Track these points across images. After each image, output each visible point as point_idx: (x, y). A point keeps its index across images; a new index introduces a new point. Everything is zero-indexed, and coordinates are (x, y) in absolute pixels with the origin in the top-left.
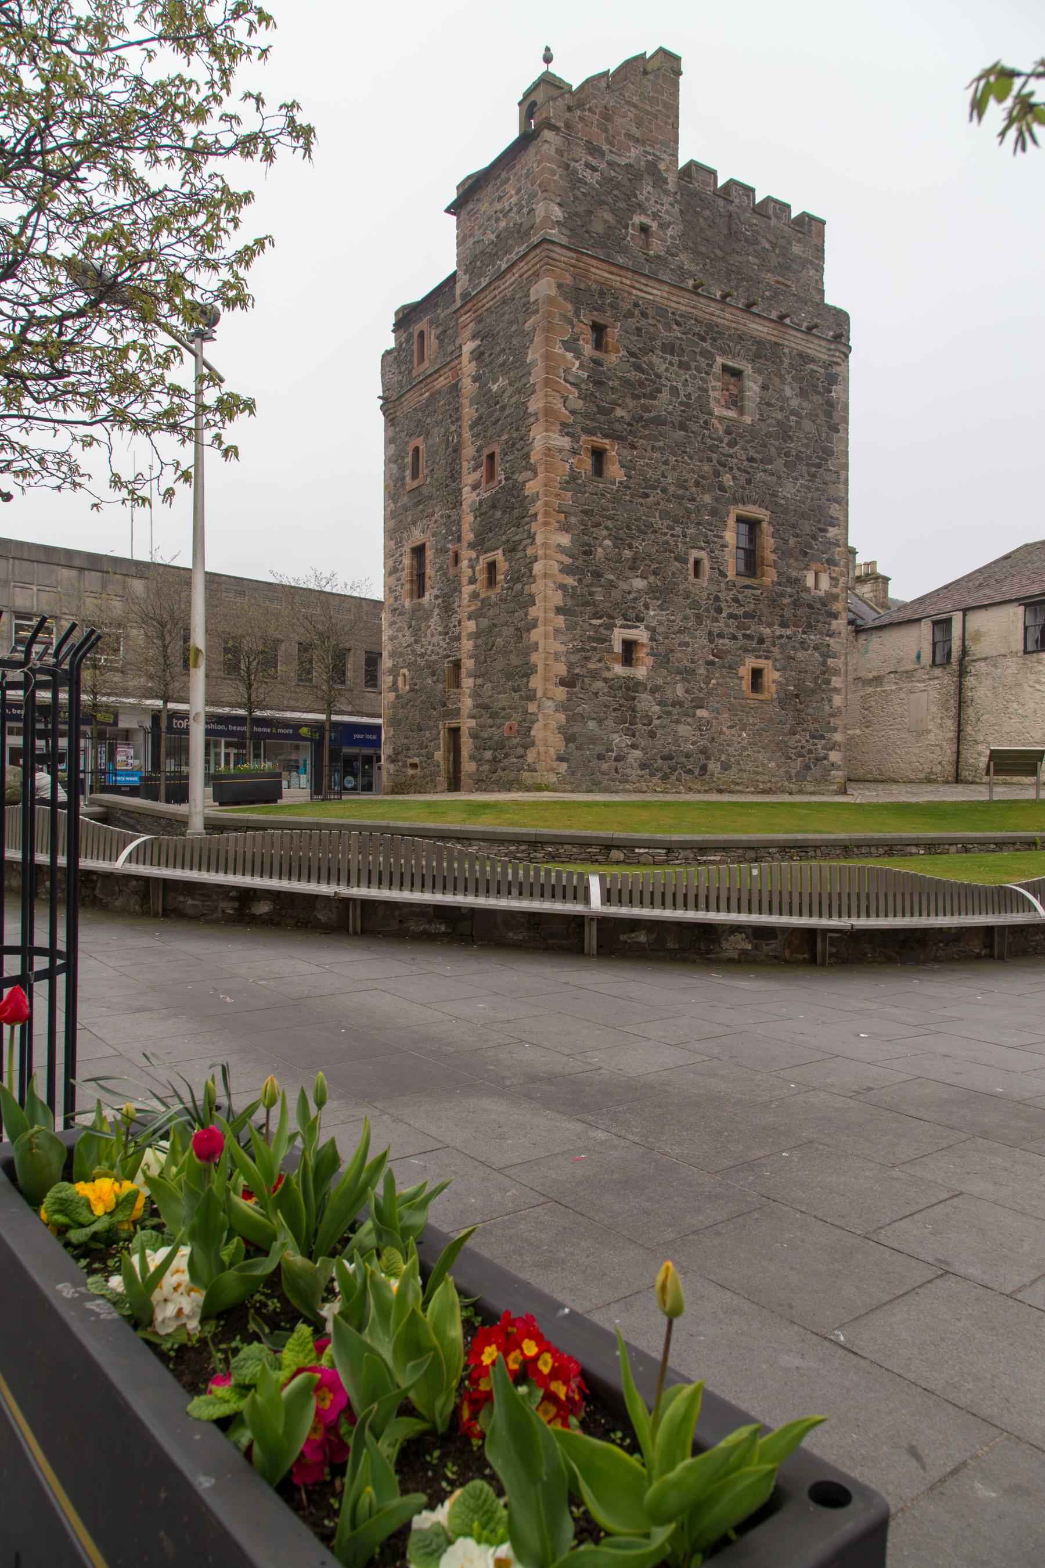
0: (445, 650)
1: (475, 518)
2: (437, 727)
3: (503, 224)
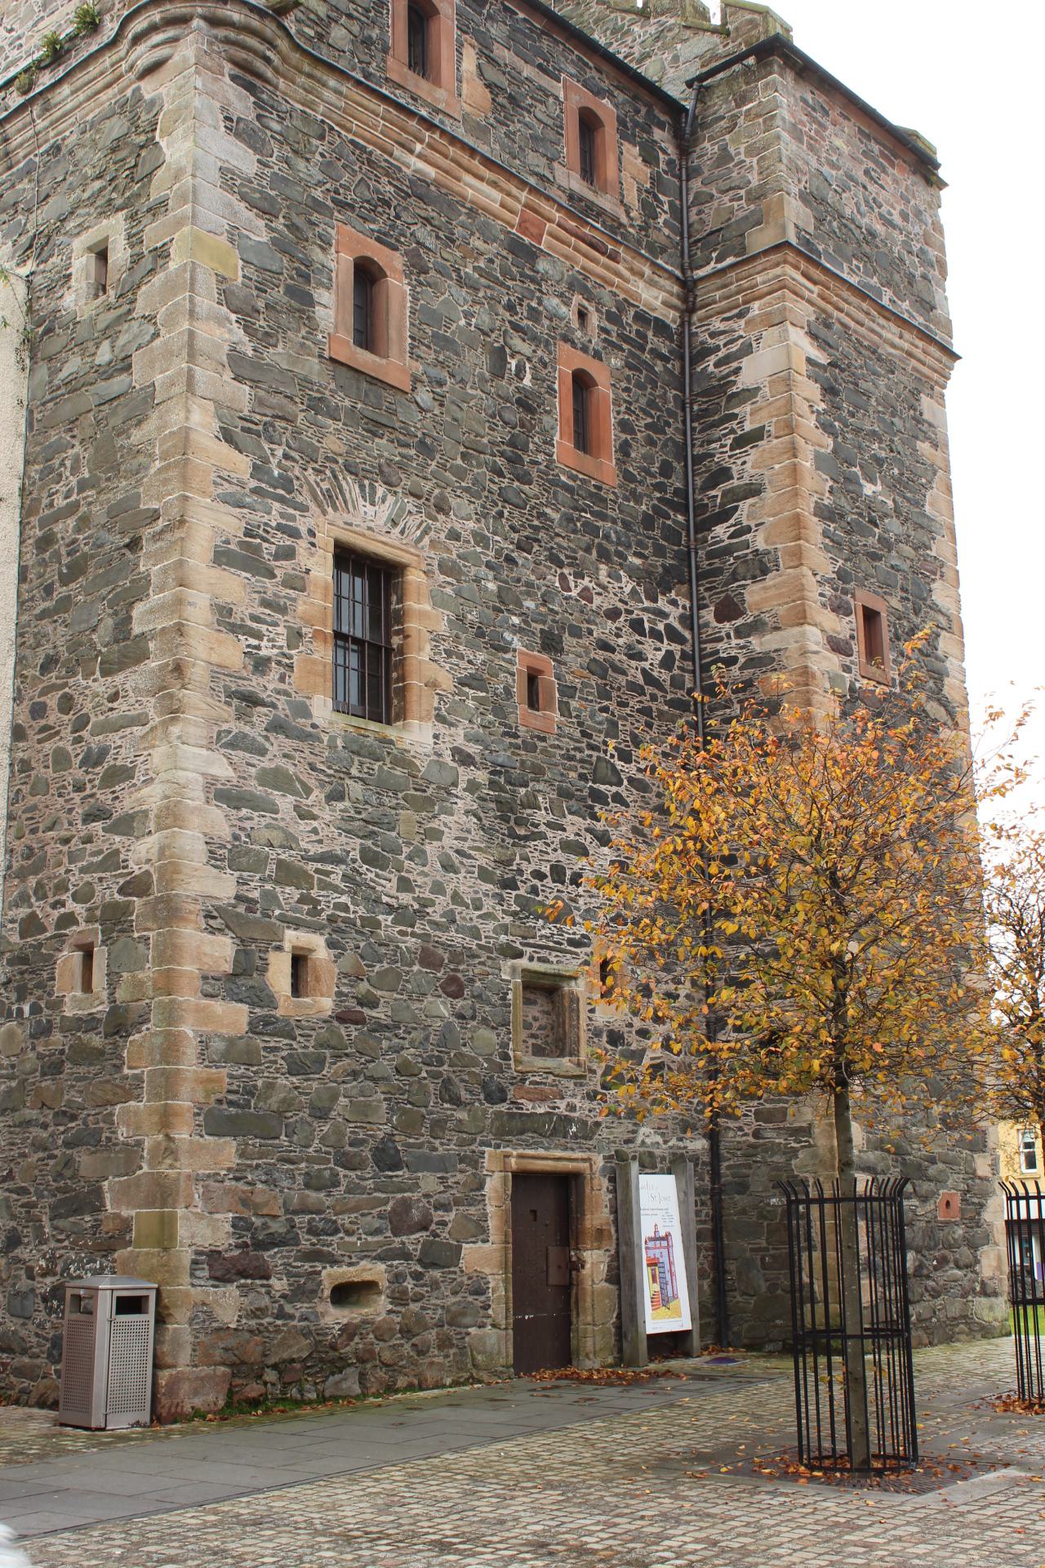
0: (505, 929)
2: (474, 1161)
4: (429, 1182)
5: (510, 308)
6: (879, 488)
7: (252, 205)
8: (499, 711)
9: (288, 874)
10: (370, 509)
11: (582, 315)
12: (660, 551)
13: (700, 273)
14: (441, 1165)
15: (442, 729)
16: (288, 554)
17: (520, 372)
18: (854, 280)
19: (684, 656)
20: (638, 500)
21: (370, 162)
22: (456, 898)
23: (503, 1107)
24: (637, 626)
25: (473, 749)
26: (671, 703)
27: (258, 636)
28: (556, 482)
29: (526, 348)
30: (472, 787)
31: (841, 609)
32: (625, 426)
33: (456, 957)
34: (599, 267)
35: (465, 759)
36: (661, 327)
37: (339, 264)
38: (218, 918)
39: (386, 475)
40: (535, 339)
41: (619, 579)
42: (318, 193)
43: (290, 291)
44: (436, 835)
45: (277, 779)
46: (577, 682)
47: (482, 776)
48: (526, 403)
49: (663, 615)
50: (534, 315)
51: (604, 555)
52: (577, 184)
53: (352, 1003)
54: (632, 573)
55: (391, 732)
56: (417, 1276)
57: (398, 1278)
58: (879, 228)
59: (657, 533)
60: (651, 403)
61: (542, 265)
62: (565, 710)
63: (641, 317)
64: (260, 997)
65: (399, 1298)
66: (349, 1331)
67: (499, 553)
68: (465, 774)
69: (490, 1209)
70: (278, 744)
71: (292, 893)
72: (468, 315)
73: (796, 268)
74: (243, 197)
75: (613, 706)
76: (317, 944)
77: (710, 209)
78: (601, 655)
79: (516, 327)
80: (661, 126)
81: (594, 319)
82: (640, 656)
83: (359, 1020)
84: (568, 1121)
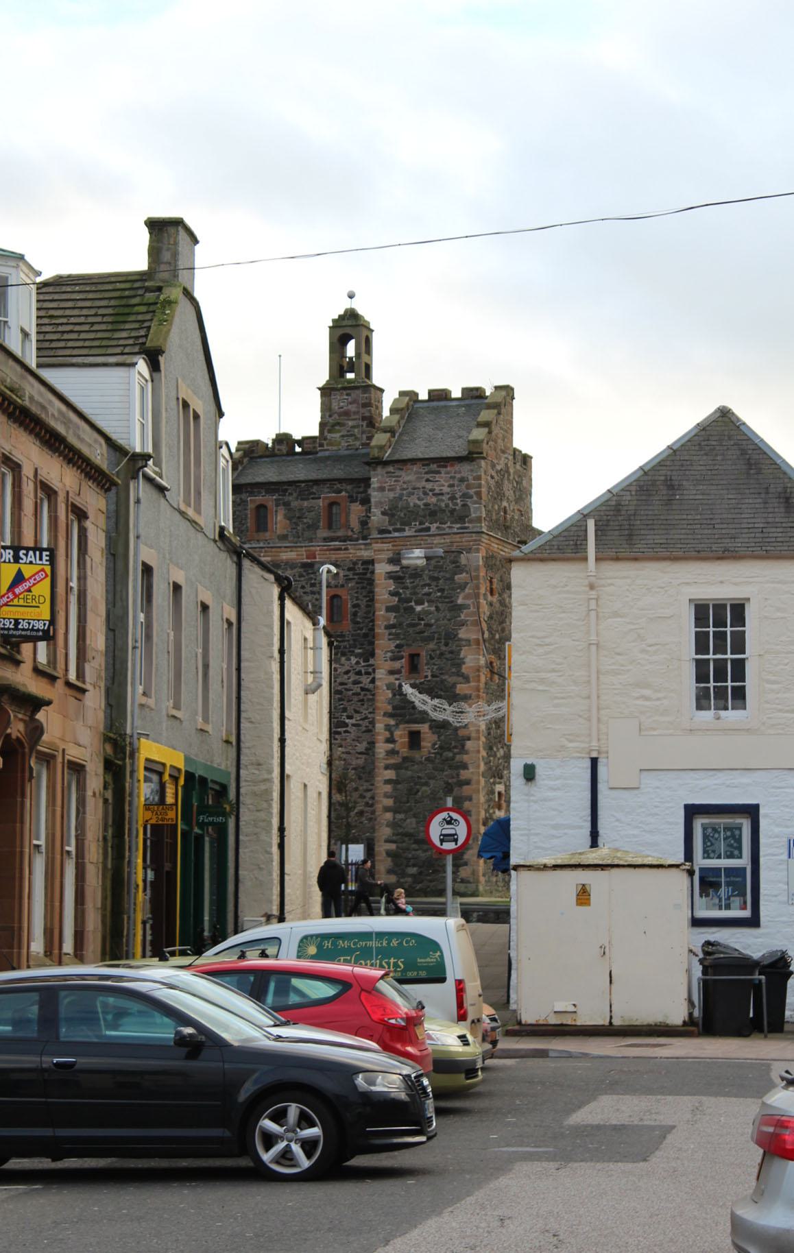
1: (394, 695)
3: (434, 500)
5: (303, 587)
20: (361, 629)
24: (359, 673)
29: (310, 597)
32: (354, 606)
51: (343, 654)
82: (360, 683)
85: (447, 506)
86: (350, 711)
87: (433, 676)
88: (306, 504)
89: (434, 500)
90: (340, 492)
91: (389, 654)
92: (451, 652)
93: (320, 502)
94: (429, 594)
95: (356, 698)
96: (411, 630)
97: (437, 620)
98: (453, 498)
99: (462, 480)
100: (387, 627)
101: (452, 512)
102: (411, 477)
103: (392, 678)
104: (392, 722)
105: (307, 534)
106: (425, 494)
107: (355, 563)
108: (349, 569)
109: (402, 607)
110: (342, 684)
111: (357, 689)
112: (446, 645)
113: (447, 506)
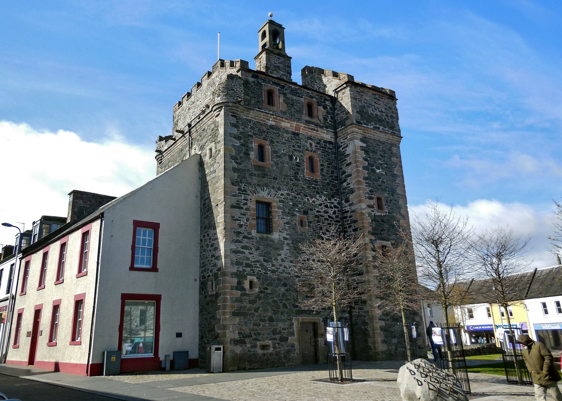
1: (372, 221)
2: (291, 320)
4: (281, 325)
5: (293, 146)
6: (381, 170)
7: (236, 139)
8: (294, 229)
9: (248, 265)
10: (263, 193)
11: (311, 144)
12: (331, 190)
13: (338, 130)
14: (284, 321)
15: (281, 233)
16: (246, 204)
17: (296, 159)
18: (372, 127)
19: (338, 211)
20: (326, 180)
21: (261, 125)
22: (285, 267)
23: (297, 309)
24: (326, 206)
25: (288, 237)
26: (335, 221)
27: (240, 220)
28: (306, 180)
29: (297, 154)
30: (288, 244)
31: (371, 198)
32: (322, 165)
33: (285, 279)
34: (314, 133)
35: (285, 239)
36: (330, 143)
37: (254, 145)
38: (234, 275)
39: (267, 185)
40: (300, 151)
41: (321, 197)
42: (250, 133)
43: (244, 153)
44: (280, 255)
45: (245, 247)
46: (312, 220)
47: (290, 242)
48: (298, 165)
49: (333, 203)
50: (299, 147)
51: (318, 193)
52: (307, 118)
53: (262, 289)
54: (325, 195)
55: (269, 236)
56: (278, 343)
57: (274, 344)
58: (379, 114)
59: (331, 186)
60: (328, 159)
61: (300, 136)
62: (309, 226)
63: (325, 142)
64: (243, 289)
65: (275, 348)
66: (264, 355)
67: (292, 196)
68: (286, 242)
69: (295, 329)
70: (245, 240)
71: (248, 269)
72: (284, 150)
73: (356, 128)
74: (234, 138)
75: (321, 224)
76: (255, 279)
77: (339, 116)
78: (318, 214)
79: (295, 150)
80: (328, 100)
81: (314, 145)
82: (328, 213)
83: (264, 292)
84: (313, 311)
85: (385, 119)
86: (324, 229)
87: (389, 212)
88: (295, 98)
89: (379, 114)
90: (312, 97)
91: (367, 195)
92: (395, 201)
93: (303, 100)
94: (381, 164)
95: (326, 222)
96: (376, 183)
97: (387, 181)
98: (387, 116)
99: (390, 108)
100: (365, 178)
101: (388, 122)
102: (368, 98)
103: (369, 210)
104: (373, 238)
105: (297, 115)
106: (375, 109)
107: (320, 140)
108: (317, 143)
109: (369, 168)
110: (318, 212)
111: (326, 216)
112: (393, 196)
113: (385, 119)
